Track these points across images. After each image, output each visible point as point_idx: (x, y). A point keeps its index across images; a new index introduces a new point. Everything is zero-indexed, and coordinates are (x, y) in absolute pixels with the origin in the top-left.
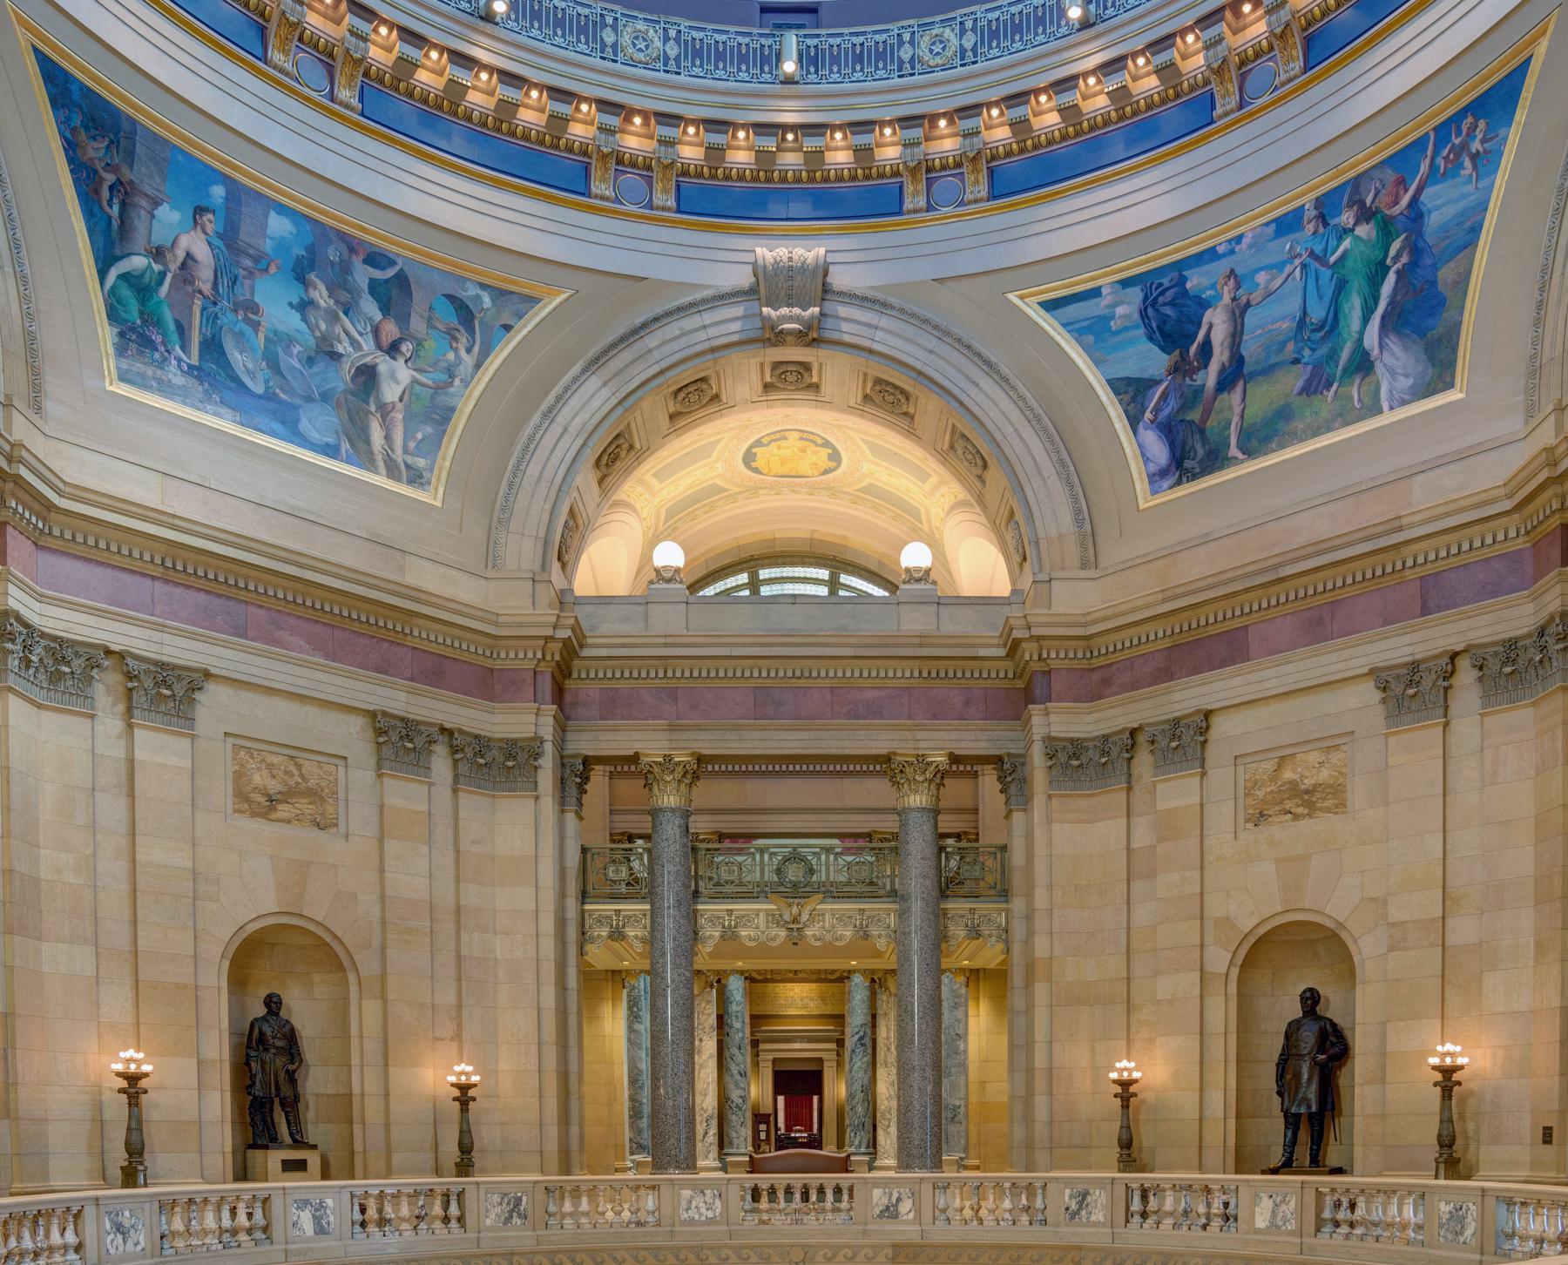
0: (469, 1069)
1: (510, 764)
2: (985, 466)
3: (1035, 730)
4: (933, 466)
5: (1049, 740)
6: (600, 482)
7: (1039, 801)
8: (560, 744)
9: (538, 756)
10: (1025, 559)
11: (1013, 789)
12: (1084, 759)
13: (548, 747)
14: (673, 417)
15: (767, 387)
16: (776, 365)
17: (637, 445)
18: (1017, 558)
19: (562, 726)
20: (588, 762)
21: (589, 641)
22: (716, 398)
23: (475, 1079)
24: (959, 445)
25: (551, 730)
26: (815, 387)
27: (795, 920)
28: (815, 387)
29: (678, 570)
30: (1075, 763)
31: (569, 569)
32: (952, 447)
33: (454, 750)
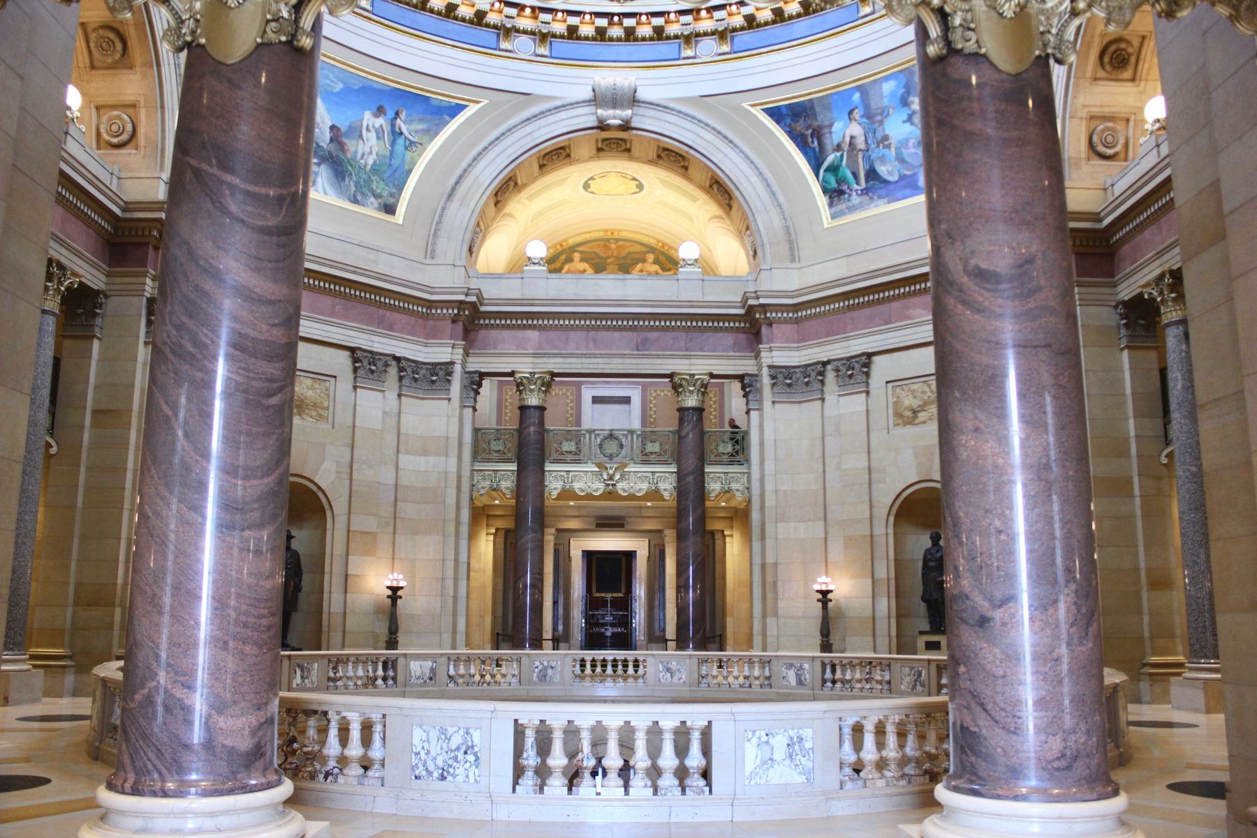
0: (401, 577)
1: (434, 378)
2: (731, 198)
3: (763, 360)
4: (702, 197)
5: (770, 367)
6: (496, 204)
7: (767, 404)
8: (463, 365)
9: (450, 374)
10: (755, 253)
11: (751, 397)
12: (794, 378)
13: (458, 368)
14: (541, 166)
15: (599, 150)
16: (604, 140)
17: (519, 183)
18: (751, 253)
19: (466, 354)
20: (483, 375)
21: (486, 301)
22: (569, 156)
23: (402, 584)
24: (715, 187)
25: (461, 357)
26: (629, 150)
27: (611, 478)
28: (629, 150)
29: (541, 259)
30: (788, 381)
31: (474, 255)
32: (711, 186)
33: (401, 370)
